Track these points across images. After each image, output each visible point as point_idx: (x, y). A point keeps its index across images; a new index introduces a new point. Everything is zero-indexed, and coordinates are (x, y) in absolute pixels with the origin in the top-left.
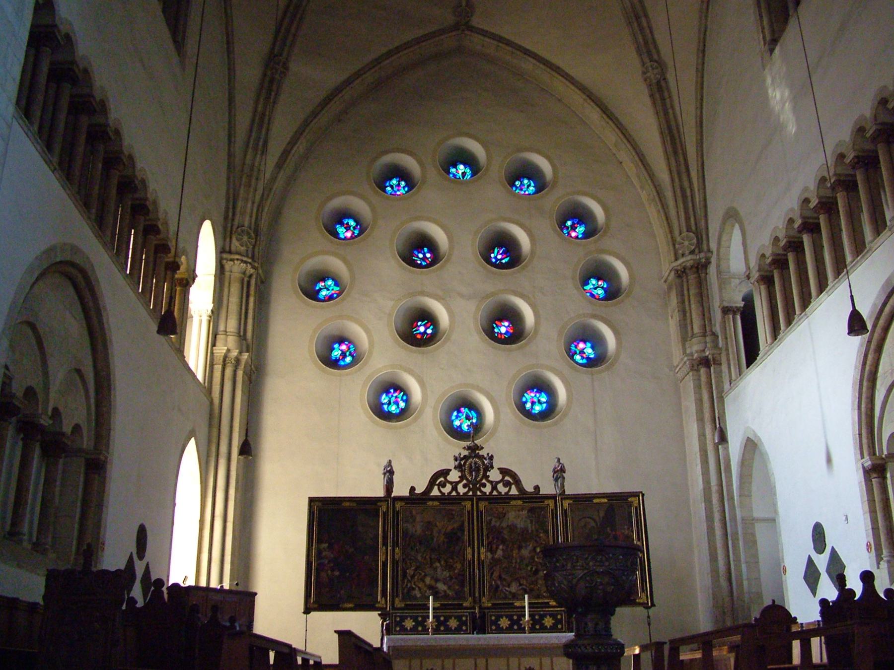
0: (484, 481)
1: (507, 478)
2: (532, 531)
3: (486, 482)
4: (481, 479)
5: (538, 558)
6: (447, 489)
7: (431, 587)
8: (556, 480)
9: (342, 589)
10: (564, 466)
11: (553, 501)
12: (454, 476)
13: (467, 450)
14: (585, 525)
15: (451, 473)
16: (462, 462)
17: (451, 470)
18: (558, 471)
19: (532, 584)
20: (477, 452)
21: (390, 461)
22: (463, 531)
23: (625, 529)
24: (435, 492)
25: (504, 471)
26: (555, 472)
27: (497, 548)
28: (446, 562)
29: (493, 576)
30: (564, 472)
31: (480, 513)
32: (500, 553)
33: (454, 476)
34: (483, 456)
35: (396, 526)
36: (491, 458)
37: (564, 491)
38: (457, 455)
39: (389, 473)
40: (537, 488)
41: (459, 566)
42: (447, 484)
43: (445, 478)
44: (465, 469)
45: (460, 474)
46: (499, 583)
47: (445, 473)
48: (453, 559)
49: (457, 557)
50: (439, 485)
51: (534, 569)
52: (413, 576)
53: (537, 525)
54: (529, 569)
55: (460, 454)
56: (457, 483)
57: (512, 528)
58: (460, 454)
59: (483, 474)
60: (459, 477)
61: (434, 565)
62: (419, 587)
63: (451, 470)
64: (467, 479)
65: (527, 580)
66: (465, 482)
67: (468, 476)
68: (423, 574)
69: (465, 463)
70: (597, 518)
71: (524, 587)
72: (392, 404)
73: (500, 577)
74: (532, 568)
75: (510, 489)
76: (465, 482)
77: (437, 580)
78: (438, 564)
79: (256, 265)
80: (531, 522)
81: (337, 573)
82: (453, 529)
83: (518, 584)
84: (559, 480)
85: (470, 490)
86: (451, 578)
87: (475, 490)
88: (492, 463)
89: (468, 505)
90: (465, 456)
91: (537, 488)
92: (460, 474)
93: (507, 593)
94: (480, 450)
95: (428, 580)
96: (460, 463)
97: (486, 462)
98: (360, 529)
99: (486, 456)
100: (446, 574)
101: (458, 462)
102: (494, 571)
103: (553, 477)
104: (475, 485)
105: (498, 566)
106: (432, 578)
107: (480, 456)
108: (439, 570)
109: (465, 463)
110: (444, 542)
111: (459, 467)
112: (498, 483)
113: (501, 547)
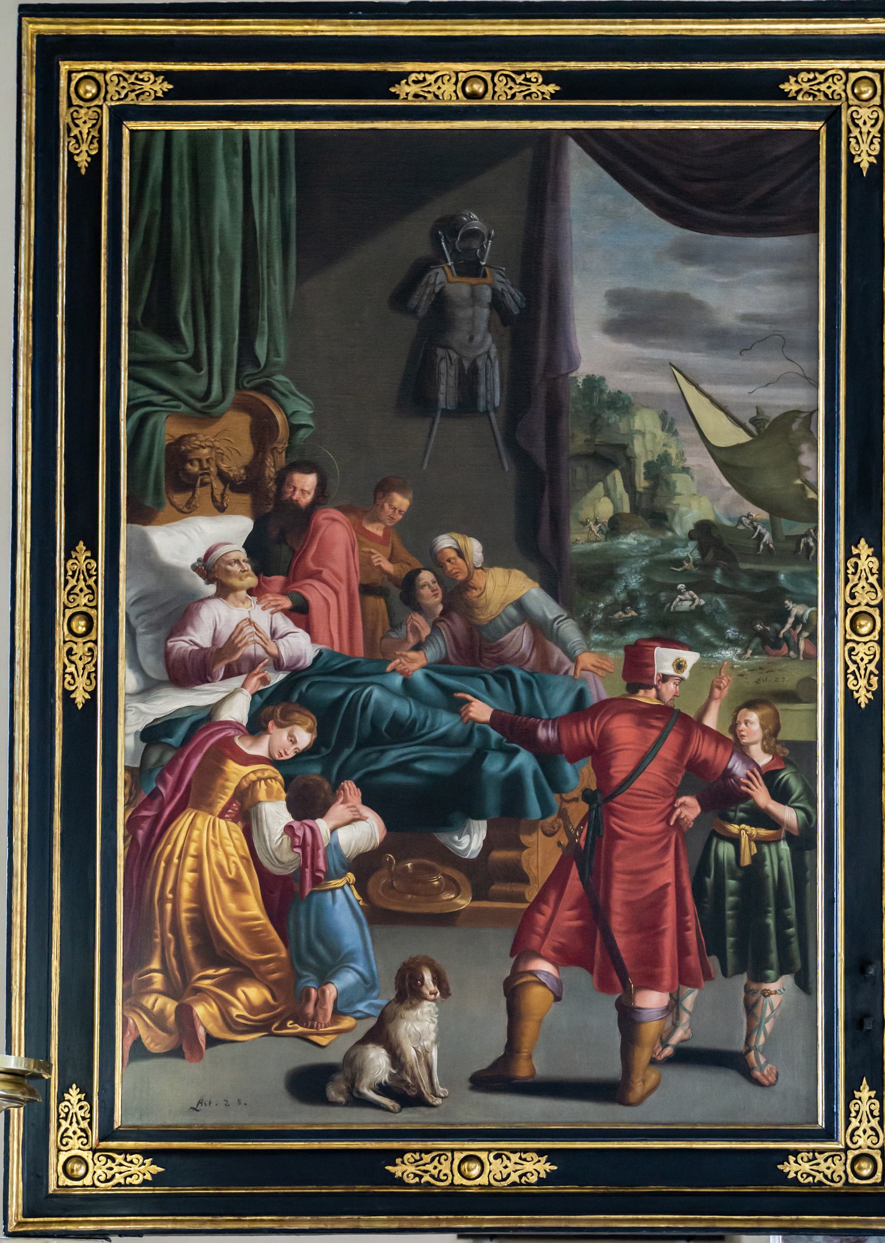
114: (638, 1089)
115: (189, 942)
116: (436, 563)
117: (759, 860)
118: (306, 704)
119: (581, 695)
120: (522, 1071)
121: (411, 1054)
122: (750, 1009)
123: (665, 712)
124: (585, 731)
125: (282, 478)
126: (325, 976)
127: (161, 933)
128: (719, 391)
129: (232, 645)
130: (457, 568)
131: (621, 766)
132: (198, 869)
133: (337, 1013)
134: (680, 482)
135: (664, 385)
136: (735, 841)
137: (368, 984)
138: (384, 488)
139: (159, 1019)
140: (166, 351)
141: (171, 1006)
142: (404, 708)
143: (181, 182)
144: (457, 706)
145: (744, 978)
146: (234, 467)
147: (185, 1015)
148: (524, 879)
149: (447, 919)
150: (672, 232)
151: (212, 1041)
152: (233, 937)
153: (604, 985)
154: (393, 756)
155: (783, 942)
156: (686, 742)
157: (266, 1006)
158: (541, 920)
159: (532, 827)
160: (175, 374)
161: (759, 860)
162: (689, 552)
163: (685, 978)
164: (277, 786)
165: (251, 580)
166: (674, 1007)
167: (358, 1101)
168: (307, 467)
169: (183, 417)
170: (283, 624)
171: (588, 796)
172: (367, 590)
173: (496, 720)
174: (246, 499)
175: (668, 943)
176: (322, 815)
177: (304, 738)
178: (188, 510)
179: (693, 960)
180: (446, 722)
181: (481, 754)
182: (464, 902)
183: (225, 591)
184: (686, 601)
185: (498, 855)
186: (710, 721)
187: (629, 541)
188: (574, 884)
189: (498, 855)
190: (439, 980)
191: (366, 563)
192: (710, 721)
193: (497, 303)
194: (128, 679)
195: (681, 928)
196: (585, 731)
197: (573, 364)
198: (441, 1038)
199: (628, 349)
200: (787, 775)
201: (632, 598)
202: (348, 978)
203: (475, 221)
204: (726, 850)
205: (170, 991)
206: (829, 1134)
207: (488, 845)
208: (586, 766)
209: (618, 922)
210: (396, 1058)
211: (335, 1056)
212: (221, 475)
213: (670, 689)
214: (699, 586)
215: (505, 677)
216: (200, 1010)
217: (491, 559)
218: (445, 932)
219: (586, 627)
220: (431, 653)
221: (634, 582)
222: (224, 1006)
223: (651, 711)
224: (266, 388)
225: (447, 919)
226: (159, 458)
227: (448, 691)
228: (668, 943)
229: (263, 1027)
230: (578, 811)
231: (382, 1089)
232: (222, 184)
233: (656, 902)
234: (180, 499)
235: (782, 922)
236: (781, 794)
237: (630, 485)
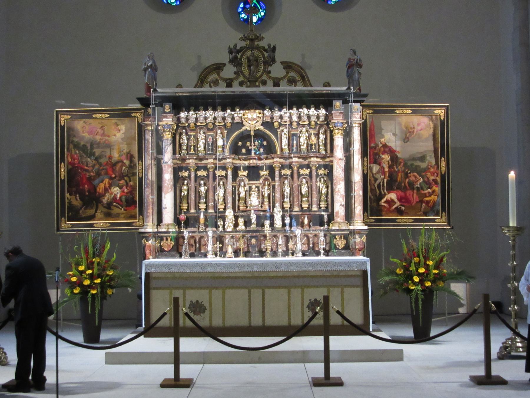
0: (264, 77)
1: (292, 74)
3: (266, 79)
4: (261, 76)
13: (244, 40)
15: (225, 68)
17: (225, 65)
25: (288, 66)
26: (350, 66)
34: (264, 47)
36: (274, 49)
38: (232, 47)
43: (218, 74)
45: (235, 69)
47: (218, 67)
55: (235, 46)
58: (235, 46)
60: (235, 73)
63: (225, 65)
64: (244, 76)
66: (241, 78)
69: (242, 56)
76: (241, 78)
88: (274, 56)
90: (241, 48)
92: (235, 69)
94: (260, 40)
96: (236, 57)
97: (266, 55)
99: (266, 47)
107: (260, 47)
109: (242, 56)
111: (235, 61)
112: (280, 79)
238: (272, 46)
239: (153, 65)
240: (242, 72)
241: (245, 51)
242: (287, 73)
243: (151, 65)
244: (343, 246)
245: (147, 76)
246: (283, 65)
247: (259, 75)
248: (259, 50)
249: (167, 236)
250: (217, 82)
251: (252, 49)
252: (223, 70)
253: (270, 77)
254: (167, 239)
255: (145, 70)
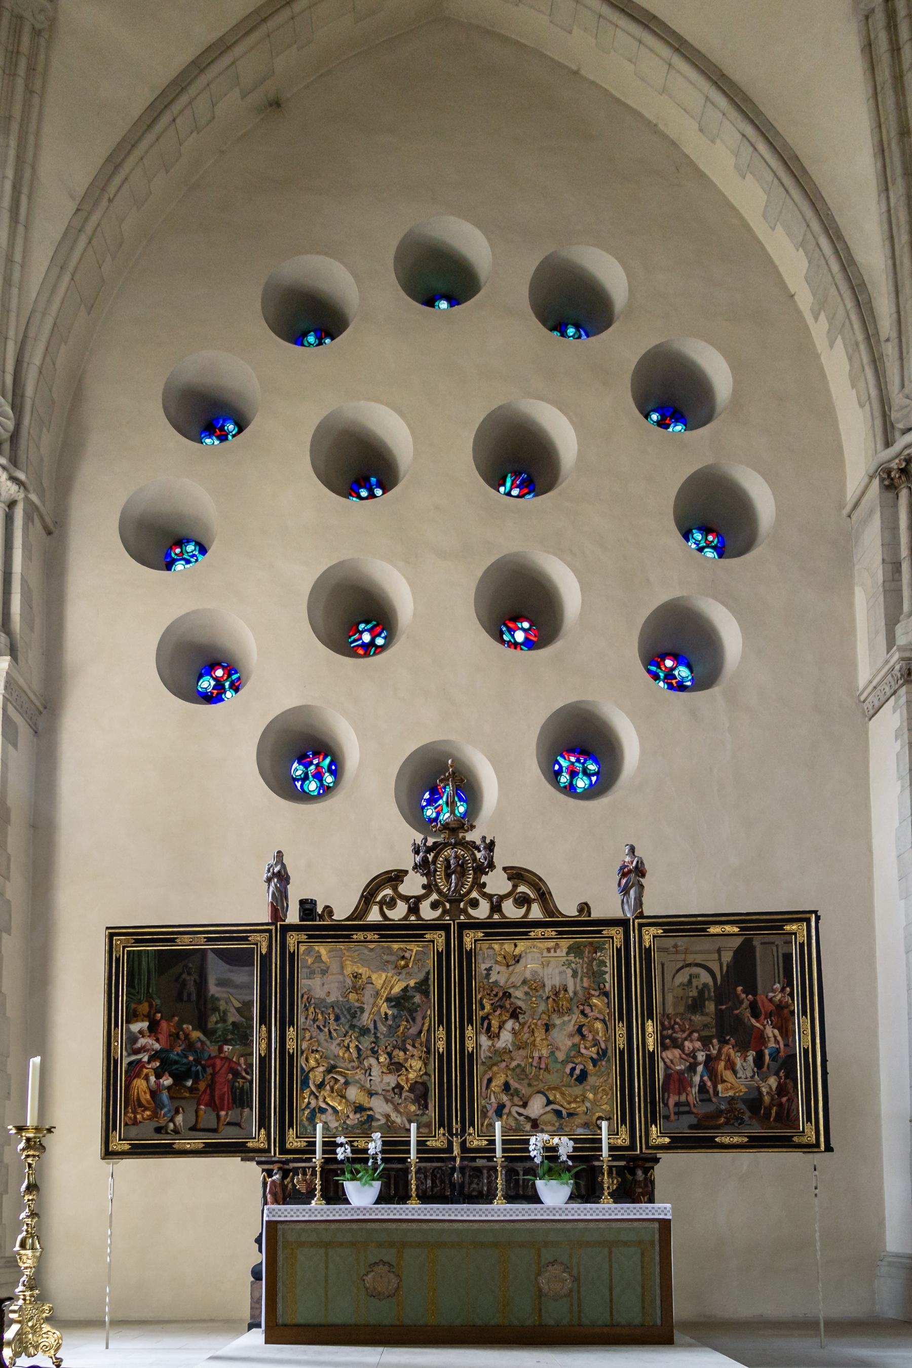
0: (474, 894)
1: (522, 889)
2: (575, 993)
3: (478, 897)
4: (469, 892)
5: (586, 1048)
6: (399, 912)
7: (359, 1109)
8: (625, 891)
9: (177, 1112)
10: (642, 863)
11: (621, 929)
12: (413, 885)
14: (690, 981)
16: (430, 857)
17: (406, 872)
18: (630, 872)
19: (575, 1101)
20: (461, 835)
21: (279, 852)
22: (426, 993)
23: (773, 991)
24: (374, 916)
25: (516, 875)
26: (624, 872)
27: (500, 1028)
28: (389, 1055)
29: (493, 1084)
30: (643, 875)
31: (467, 958)
32: (506, 1039)
33: (413, 885)
35: (289, 985)
36: (491, 847)
37: (642, 912)
39: (281, 878)
40: (584, 908)
41: (417, 1064)
42: (398, 901)
43: (395, 889)
44: (436, 871)
45: (424, 880)
46: (505, 1098)
47: (395, 877)
48: (405, 1050)
49: (414, 1046)
50: (381, 903)
51: (577, 1072)
52: (321, 1086)
53: (585, 979)
54: (568, 1070)
56: (419, 899)
57: (533, 985)
59: (474, 878)
60: (424, 887)
61: (366, 1063)
62: (333, 1108)
63: (406, 872)
64: (439, 892)
65: (562, 1094)
66: (434, 896)
67: (441, 883)
68: (342, 1080)
70: (715, 968)
71: (560, 1108)
72: (311, 778)
73: (506, 1087)
74: (573, 1069)
75: (528, 910)
76: (434, 896)
77: (371, 1094)
78: (373, 1061)
79: (22, 476)
80: (575, 974)
81: (167, 1081)
82: (405, 990)
83: (544, 1100)
84: (632, 892)
85: (445, 912)
86: (399, 1086)
87: (455, 911)
88: (492, 857)
89: (439, 938)
90: (434, 843)
91: (584, 908)
92: (424, 880)
93: (522, 1118)
94: (467, 831)
95: (353, 1093)
96: (425, 860)
97: (479, 855)
98: (213, 989)
99: (478, 842)
100: (391, 1080)
101: (421, 854)
102: (495, 1074)
103: (619, 885)
104: (455, 902)
105: (503, 1065)
106: (362, 1088)
107: (468, 843)
108: (376, 1071)
110: (386, 1014)
111: (423, 867)
112: (502, 898)
113: (509, 1025)
114: (220, 1130)
115: (136, 1103)
116: (183, 1030)
117: (243, 1086)
118: (158, 1058)
119: (210, 1055)
120: (198, 1126)
121: (178, 1124)
122: (241, 1115)
123: (226, 1058)
124: (211, 1062)
125: (155, 1014)
126: (161, 1109)
127: (131, 1102)
128: (239, 997)
129: (144, 1047)
130: (187, 1031)
131: (217, 1068)
132: (138, 1089)
133: (164, 1116)
134: (229, 1014)
135: (225, 995)
136: (239, 1082)
137: (169, 1111)
138: (173, 1016)
139: (130, 1118)
140: (132, 991)
141: (133, 1116)
142: (176, 1058)
143: (136, 959)
144: (187, 1057)
145: (240, 1109)
146: (145, 1013)
147: (135, 1117)
148: (199, 1090)
149: (185, 1098)
150: (227, 967)
151: (140, 1122)
152: (144, 1102)
153: (214, 1110)
154: (174, 1067)
155: (248, 1102)
156: (230, 1063)
157: (150, 1115)
158: (202, 1098)
159: (200, 1080)
160: (135, 995)
161: (243, 1086)
162: (230, 1027)
163: (229, 1109)
164: (153, 1073)
165: (148, 1034)
166: (227, 1114)
167: (167, 1133)
168: (159, 1013)
169: (135, 1003)
170: (154, 1042)
171: (211, 1074)
172: (170, 1035)
173: (194, 1060)
174: (147, 1019)
175: (226, 1102)
176: (161, 1078)
177: (158, 1064)
178: (137, 1021)
179: (231, 1105)
180: (185, 1061)
181: (191, 1067)
182: (187, 1095)
183: (143, 1036)
184: (230, 1037)
185: (194, 1086)
186: (234, 1060)
187: (219, 1025)
188: (208, 1091)
189: (194, 1086)
190: (183, 1110)
191: (170, 1031)
192: (234, 1060)
193: (195, 981)
194: (124, 1053)
195: (228, 1099)
196: (211, 1062)
197: (209, 991)
198: (183, 1120)
199: (220, 989)
200: (249, 1070)
201: (220, 1036)
202: (166, 1110)
203: (191, 965)
204: (237, 1084)
205: (133, 1112)
206: (255, 1138)
207: (192, 1084)
208: (211, 1068)
209: (216, 1098)
210: (175, 1125)
211: (162, 1125)
212: (143, 1015)
213: (227, 1053)
214: (232, 1033)
215: (196, 1052)
216: (138, 1116)
217: (193, 1029)
218: (183, 1101)
219: (211, 1042)
220: (181, 1048)
221: (220, 1033)
222: (142, 1115)
223: (223, 1058)
224: (151, 998)
225: (185, 1098)
226: (131, 1011)
227: (185, 1055)
228: (226, 1102)
229: (150, 1119)
230: (209, 1077)
231: (172, 1131)
232: (143, 959)
233: (224, 1094)
234: (135, 1019)
235: (247, 1098)
236: (247, 1073)
237: (219, 1014)
238: (488, 841)
239: (283, 872)
240: (436, 885)
241: (442, 849)
242: (515, 887)
243: (279, 872)
244: (615, 1187)
245: (271, 889)
246: (507, 873)
247: (465, 890)
248: (466, 847)
249: (304, 1169)
250: (393, 902)
251: (454, 846)
252: (402, 881)
253: (485, 895)
254: (305, 1174)
255: (269, 880)
